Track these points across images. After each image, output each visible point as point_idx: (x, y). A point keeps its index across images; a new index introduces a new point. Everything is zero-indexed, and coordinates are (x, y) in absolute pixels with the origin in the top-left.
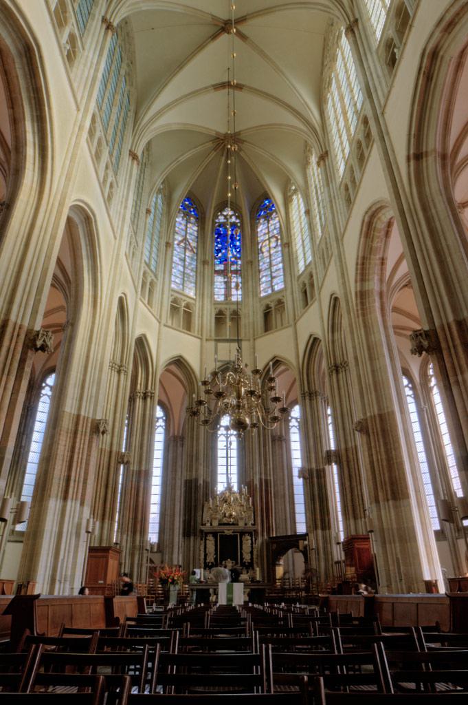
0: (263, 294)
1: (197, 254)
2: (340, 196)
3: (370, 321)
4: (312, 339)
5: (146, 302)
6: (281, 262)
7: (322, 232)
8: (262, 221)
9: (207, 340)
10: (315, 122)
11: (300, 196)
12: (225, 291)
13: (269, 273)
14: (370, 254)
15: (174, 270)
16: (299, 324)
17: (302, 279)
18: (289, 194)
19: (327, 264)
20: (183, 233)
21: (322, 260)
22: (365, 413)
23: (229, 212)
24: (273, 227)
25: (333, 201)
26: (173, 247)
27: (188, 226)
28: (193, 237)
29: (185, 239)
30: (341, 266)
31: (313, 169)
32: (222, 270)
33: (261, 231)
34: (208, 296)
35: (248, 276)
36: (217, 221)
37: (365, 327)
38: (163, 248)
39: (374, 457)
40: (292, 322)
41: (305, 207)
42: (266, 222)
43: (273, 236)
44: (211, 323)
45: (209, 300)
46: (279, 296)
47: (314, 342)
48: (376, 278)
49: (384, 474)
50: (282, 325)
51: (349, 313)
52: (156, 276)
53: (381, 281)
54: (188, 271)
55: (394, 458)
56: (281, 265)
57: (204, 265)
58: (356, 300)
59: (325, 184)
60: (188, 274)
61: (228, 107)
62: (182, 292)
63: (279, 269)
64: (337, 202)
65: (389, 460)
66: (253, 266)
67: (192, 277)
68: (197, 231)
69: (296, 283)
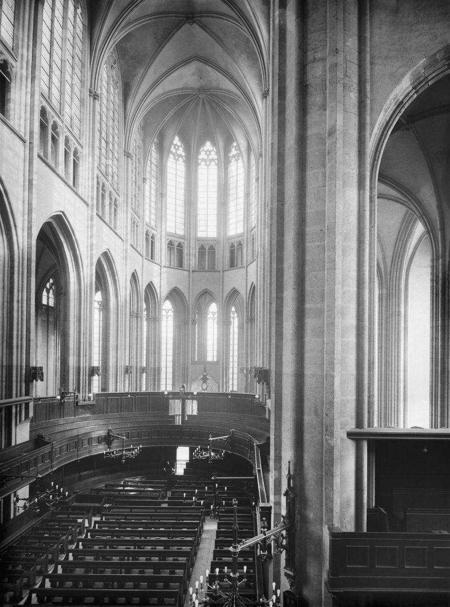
16: (249, 267)
17: (252, 232)
46: (240, 239)
47: (253, 289)
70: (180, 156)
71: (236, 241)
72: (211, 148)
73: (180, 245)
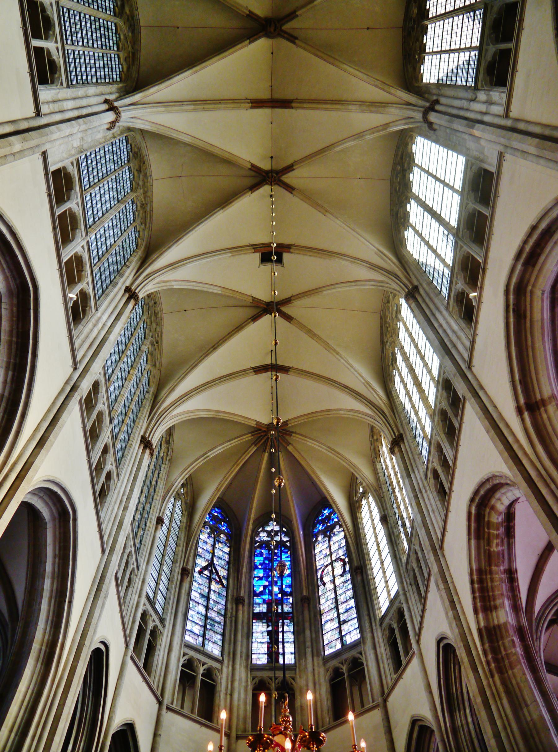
0: (328, 651)
1: (227, 588)
2: (428, 488)
3: (514, 682)
4: (416, 729)
5: (141, 664)
6: (353, 598)
7: (409, 544)
8: (320, 538)
9: (238, 738)
10: (381, 402)
11: (371, 499)
12: (268, 648)
13: (336, 615)
14: (490, 565)
15: (191, 612)
16: (391, 699)
17: (387, 620)
18: (356, 499)
19: (423, 590)
20: (209, 556)
21: (414, 587)
23: (273, 526)
24: (337, 545)
25: (419, 495)
26: (192, 577)
27: (217, 546)
28: (223, 562)
29: (211, 565)
30: (448, 589)
31: (385, 461)
32: (264, 613)
33: (321, 551)
34: (241, 656)
35: (303, 620)
36: (257, 539)
37: (509, 692)
38: (177, 576)
40: (380, 700)
41: (380, 512)
42: (327, 539)
43: (339, 559)
44: (245, 704)
45: (244, 662)
46: (354, 653)
48: (507, 603)
50: (363, 706)
51: (475, 669)
52: (162, 620)
53: (516, 607)
54: (212, 614)
56: (352, 603)
57: (237, 604)
58: (483, 644)
59: (405, 475)
60: (212, 619)
61: (272, 394)
62: (202, 649)
63: (352, 607)
64: (425, 495)
66: (311, 606)
67: (220, 623)
68: (229, 554)
70: (223, 532)
71: (346, 661)
72: (277, 528)
73: (209, 673)
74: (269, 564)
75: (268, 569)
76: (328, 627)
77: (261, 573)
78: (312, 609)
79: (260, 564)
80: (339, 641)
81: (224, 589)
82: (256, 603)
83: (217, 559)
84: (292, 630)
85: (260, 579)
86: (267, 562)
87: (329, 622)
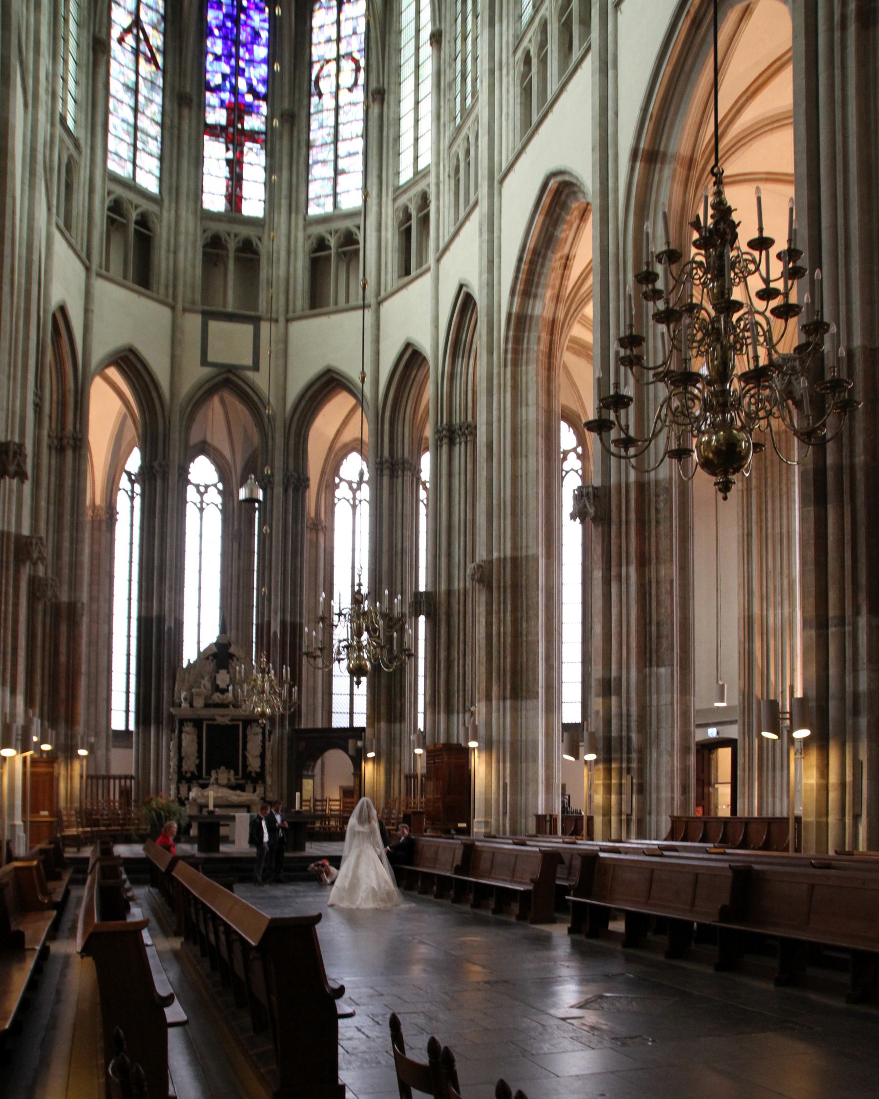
0: (314, 211)
4: (409, 352)
13: (331, 157)
22: (490, 551)
29: (137, 22)
32: (221, 127)
39: (494, 628)
46: (349, 224)
49: (505, 658)
55: (524, 632)
65: (516, 635)
69: (390, 203)
71: (336, 231)
74: (232, 29)
75: (231, 40)
76: (317, 171)
77: (216, 46)
78: (295, 133)
79: (218, 27)
80: (331, 199)
81: (160, 73)
82: (209, 106)
83: (146, 8)
84: (263, 164)
85: (217, 58)
86: (229, 24)
87: (320, 165)
